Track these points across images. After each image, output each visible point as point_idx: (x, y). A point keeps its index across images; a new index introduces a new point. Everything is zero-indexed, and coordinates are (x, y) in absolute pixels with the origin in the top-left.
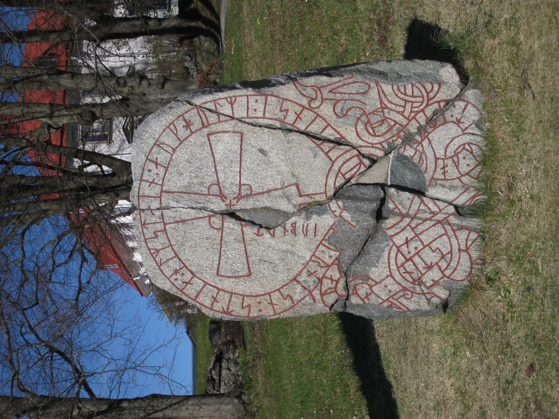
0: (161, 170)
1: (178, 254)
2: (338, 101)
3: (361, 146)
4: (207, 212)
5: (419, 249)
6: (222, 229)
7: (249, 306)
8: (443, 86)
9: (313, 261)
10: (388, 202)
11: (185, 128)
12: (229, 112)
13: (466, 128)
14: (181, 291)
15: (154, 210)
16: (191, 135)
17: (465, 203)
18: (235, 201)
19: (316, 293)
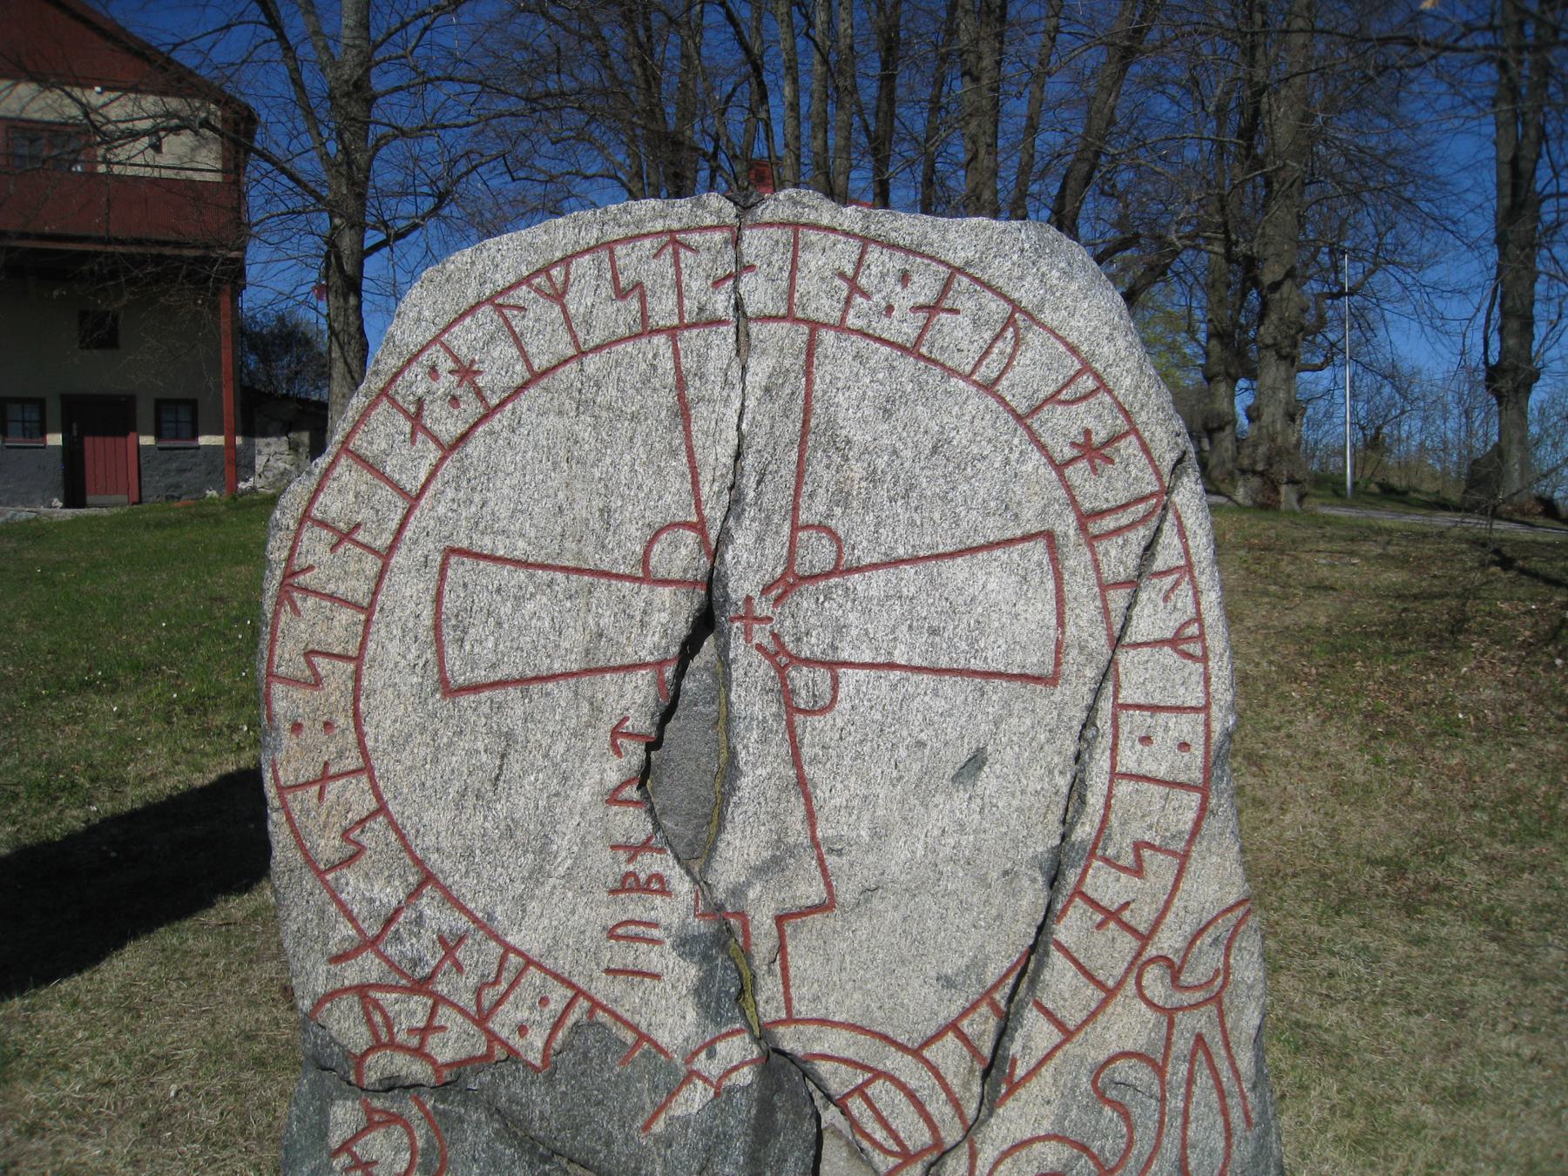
0: (904, 328)
1: (544, 382)
2: (1160, 1071)
3: (973, 1156)
4: (719, 515)
6: (646, 576)
7: (317, 682)
9: (503, 959)
11: (1081, 440)
14: (384, 392)
15: (736, 289)
16: (1051, 460)
18: (766, 641)
19: (369, 967)
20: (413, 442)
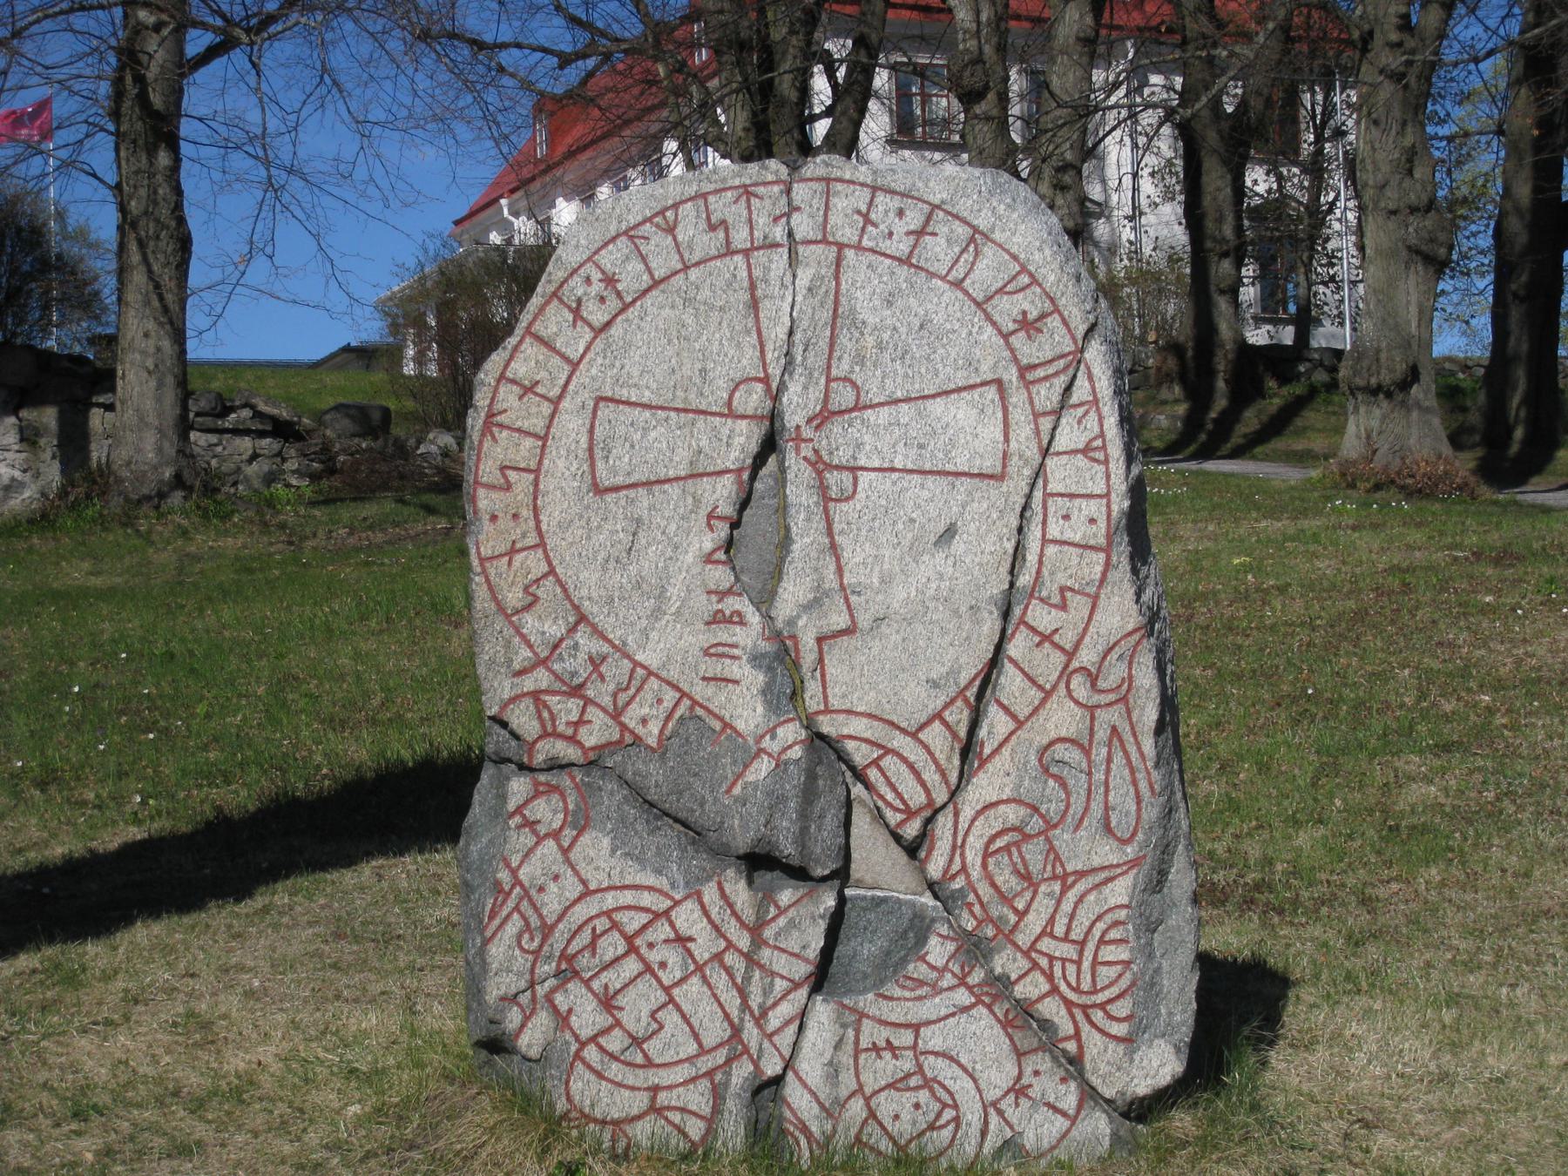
0: (901, 246)
1: (662, 287)
2: (1087, 752)
3: (956, 814)
4: (778, 372)
5: (660, 973)
6: (731, 413)
7: (508, 487)
8: (1121, 1048)
9: (633, 671)
10: (796, 888)
11: (1020, 317)
12: (1063, 441)
13: (1000, 1113)
14: (554, 294)
15: (788, 223)
16: (1000, 332)
17: (789, 1106)
18: (810, 454)
19: (541, 678)
20: (574, 326)
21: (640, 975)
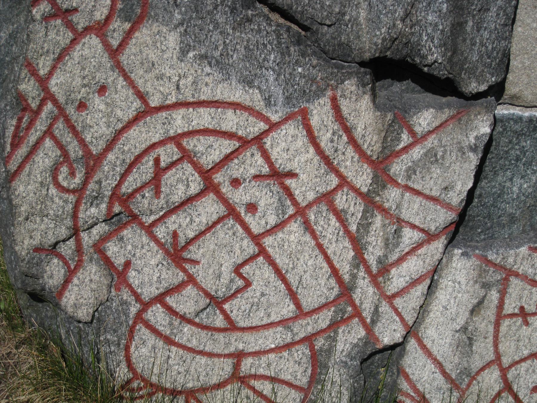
5: (248, 219)
10: (440, 108)
17: (407, 377)
21: (220, 220)
